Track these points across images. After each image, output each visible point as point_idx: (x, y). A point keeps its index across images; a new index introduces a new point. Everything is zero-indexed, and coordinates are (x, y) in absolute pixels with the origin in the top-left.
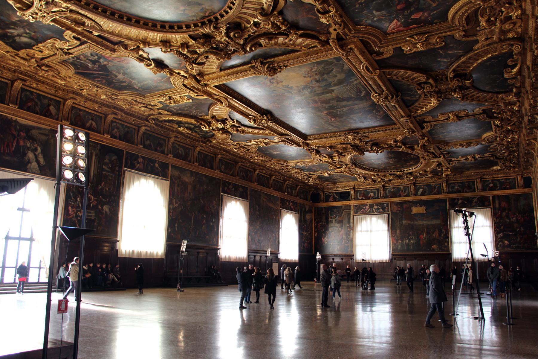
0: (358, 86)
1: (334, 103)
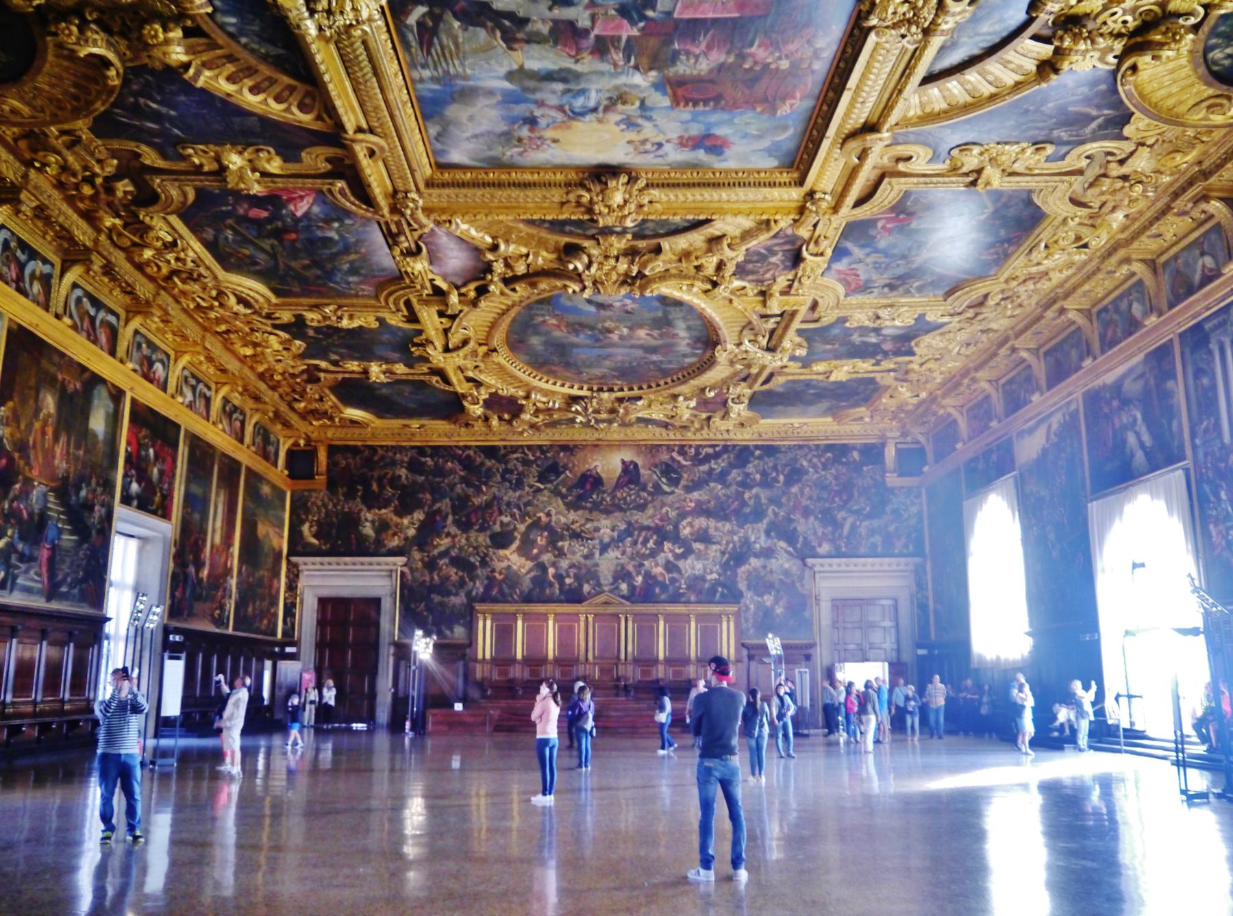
0: (420, 58)
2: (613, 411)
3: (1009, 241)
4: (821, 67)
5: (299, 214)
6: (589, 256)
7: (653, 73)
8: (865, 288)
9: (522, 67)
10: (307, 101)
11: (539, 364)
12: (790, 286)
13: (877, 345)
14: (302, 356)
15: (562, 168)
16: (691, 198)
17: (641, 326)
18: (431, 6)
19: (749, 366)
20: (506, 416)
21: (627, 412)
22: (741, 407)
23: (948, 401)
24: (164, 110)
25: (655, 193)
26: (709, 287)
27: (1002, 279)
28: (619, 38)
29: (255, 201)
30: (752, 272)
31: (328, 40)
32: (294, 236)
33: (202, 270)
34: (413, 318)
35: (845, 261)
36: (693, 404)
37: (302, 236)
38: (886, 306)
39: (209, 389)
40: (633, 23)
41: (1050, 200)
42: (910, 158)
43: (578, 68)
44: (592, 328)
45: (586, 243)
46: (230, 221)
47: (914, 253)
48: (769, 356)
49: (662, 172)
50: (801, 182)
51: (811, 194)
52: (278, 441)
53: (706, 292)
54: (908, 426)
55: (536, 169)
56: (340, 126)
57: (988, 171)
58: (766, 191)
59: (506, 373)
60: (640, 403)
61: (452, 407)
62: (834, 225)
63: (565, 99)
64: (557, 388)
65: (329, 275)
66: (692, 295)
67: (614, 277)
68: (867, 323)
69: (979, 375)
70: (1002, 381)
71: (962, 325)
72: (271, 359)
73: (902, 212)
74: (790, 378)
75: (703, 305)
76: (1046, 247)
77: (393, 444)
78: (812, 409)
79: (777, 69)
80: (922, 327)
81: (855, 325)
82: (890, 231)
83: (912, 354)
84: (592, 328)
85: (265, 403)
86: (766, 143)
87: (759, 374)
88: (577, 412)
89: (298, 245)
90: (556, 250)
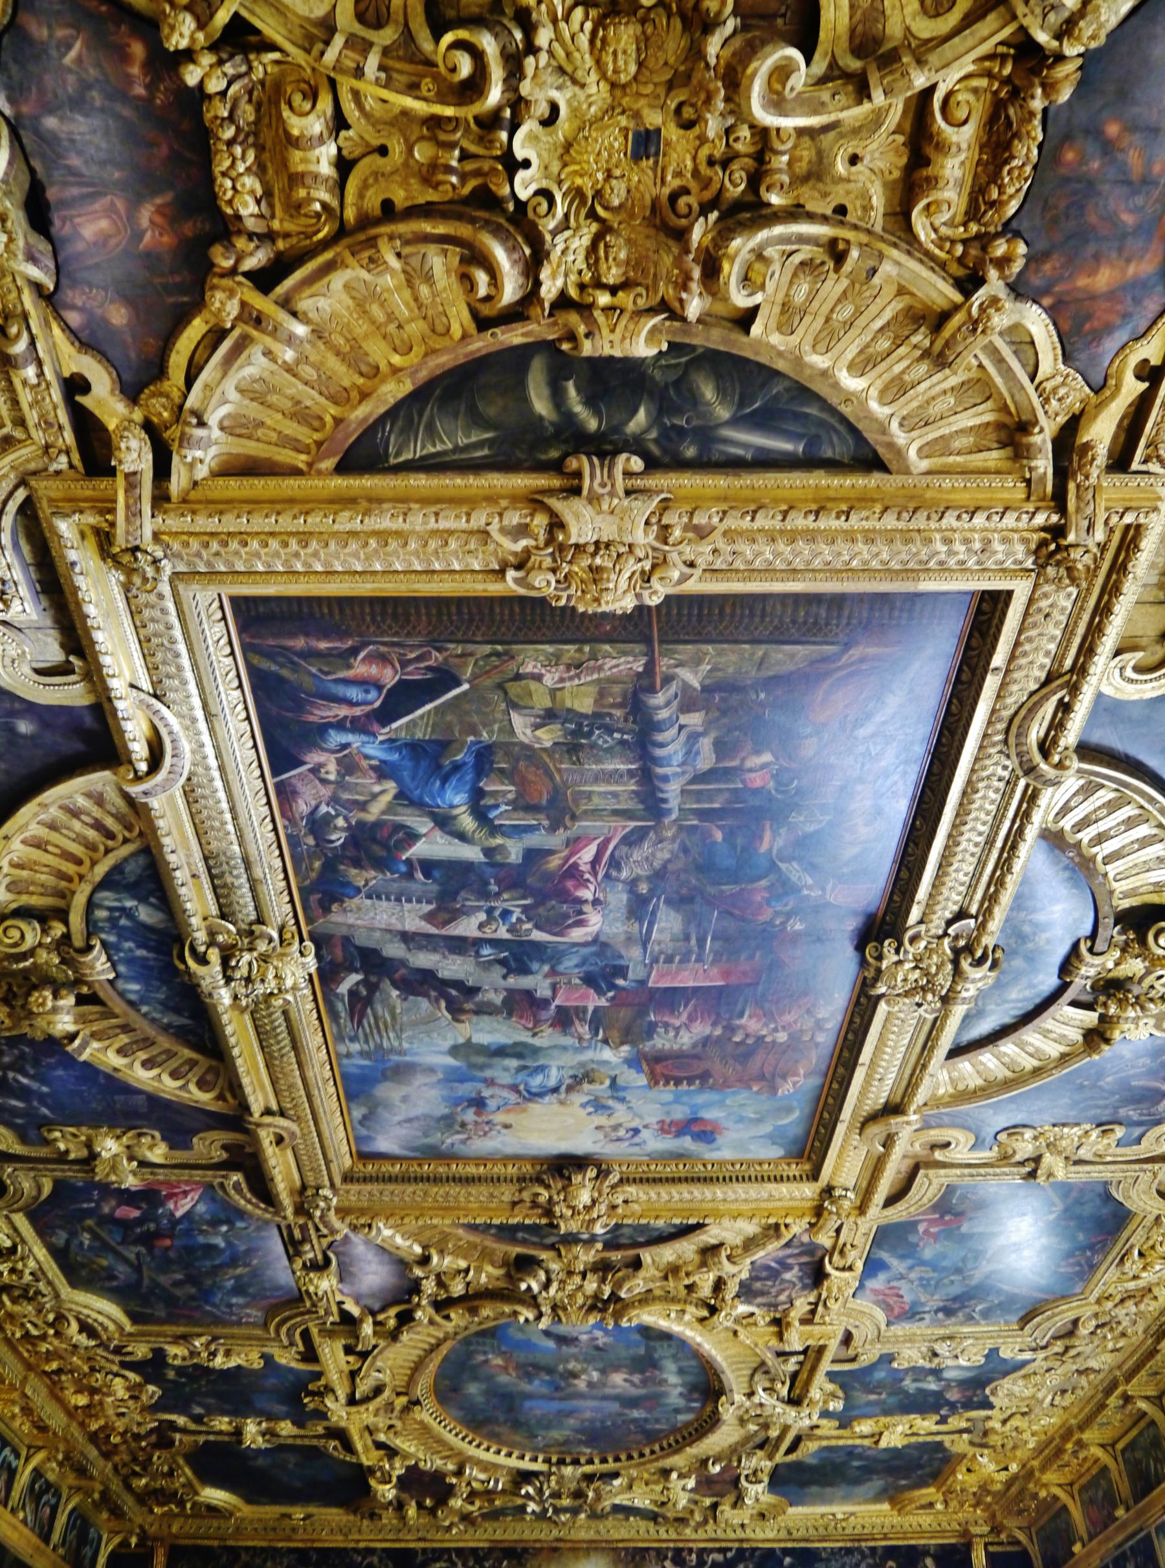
0: (349, 1029)
1: (495, 986)
2: (578, 1494)
3: (1091, 1247)
4: (826, 1039)
5: (178, 1214)
6: (547, 1272)
7: (626, 1048)
8: (912, 1314)
9: (469, 1040)
10: (209, 1077)
11: (478, 1423)
12: (813, 1312)
13: (939, 1395)
14: (154, 1408)
15: (515, 1158)
16: (676, 1197)
17: (617, 1368)
18: (366, 973)
19: (766, 1426)
20: (428, 1502)
21: (598, 1497)
22: (760, 1488)
23: (1050, 1477)
24: (35, 1085)
25: (631, 1190)
26: (705, 1313)
27: (1092, 1299)
28: (585, 1010)
29: (128, 1197)
30: (762, 1293)
31: (243, 1011)
32: (168, 1242)
33: (42, 1286)
34: (310, 1355)
35: (882, 1277)
36: (691, 1483)
37: (177, 1243)
38: (943, 1339)
39: (18, 1456)
40: (600, 992)
41: (1133, 1193)
42: (948, 1144)
43: (537, 1042)
44: (550, 1371)
45: (544, 1255)
46: (89, 1222)
47: (970, 1265)
48: (792, 1412)
49: (639, 1164)
50: (814, 1176)
51: (828, 1191)
52: (100, 1538)
53: (702, 1320)
54: (999, 1517)
55: (481, 1160)
56: (245, 1108)
57: (1048, 1159)
58: (771, 1187)
59: (432, 1438)
60: (617, 1482)
61: (351, 1487)
62: (862, 1230)
63: (521, 1077)
64: (501, 1459)
65: (206, 1295)
66: (682, 1324)
67: (580, 1300)
68: (921, 1362)
69: (1086, 1436)
70: (1120, 1446)
71: (1050, 1364)
72: (111, 1412)
73: (948, 1212)
74: (825, 1443)
75: (699, 1339)
76: (1141, 1254)
77: (264, 1544)
78: (860, 1490)
79: (774, 1042)
80: (995, 1369)
81: (906, 1365)
82: (936, 1237)
83: (991, 1406)
84: (550, 1371)
85: (92, 1478)
86: (767, 1128)
87: (780, 1438)
88: (528, 1496)
89: (172, 1254)
90: (505, 1264)
